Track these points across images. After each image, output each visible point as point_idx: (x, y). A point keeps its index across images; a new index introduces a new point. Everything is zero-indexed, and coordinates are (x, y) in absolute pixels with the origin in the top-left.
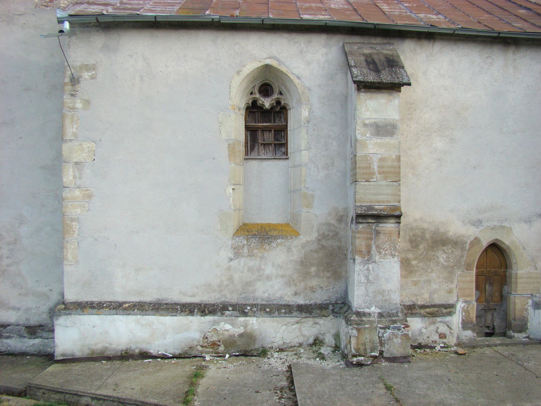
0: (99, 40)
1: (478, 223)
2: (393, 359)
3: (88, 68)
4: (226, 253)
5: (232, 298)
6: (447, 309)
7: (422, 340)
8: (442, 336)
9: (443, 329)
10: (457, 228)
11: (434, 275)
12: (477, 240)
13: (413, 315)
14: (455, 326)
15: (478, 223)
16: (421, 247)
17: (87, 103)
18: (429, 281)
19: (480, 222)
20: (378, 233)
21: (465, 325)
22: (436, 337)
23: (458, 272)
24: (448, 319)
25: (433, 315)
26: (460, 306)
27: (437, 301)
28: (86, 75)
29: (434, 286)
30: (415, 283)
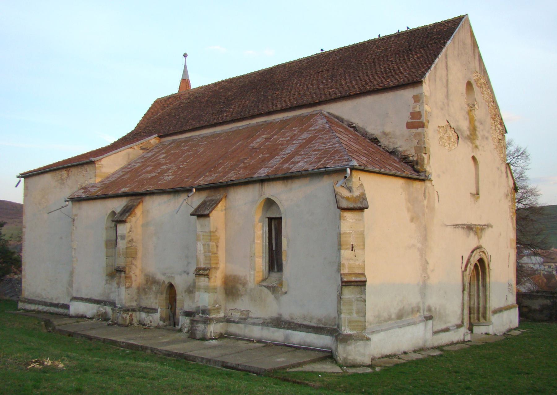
0: (77, 205)
1: (164, 274)
2: (120, 325)
3: (76, 215)
4: (104, 282)
5: (105, 299)
6: (154, 310)
7: (145, 322)
8: (151, 322)
9: (151, 319)
10: (160, 277)
11: (151, 296)
12: (164, 282)
13: (143, 311)
14: (155, 318)
15: (164, 274)
16: (149, 283)
17: (76, 228)
18: (150, 298)
19: (165, 273)
20: (121, 277)
21: (162, 319)
22: (149, 322)
23: (159, 295)
24: (152, 314)
25: (148, 312)
26: (159, 310)
27: (153, 307)
28: (76, 218)
29: (152, 300)
30: (147, 298)
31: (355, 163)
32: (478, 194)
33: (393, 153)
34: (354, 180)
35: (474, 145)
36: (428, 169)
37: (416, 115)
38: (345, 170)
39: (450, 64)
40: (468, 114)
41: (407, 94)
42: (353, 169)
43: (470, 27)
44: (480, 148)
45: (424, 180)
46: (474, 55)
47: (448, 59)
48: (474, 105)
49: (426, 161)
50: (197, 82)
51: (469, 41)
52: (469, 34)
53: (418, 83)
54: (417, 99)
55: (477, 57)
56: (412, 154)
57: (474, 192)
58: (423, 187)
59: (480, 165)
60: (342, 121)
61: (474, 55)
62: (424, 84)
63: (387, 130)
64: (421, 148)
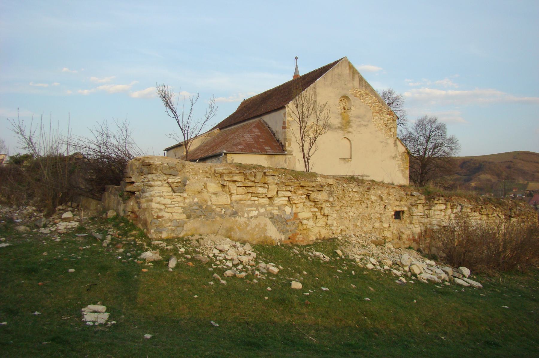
31: (225, 151)
32: (351, 158)
33: (278, 141)
34: (228, 157)
35: (345, 132)
36: (288, 148)
37: (284, 123)
38: (222, 155)
39: (318, 90)
40: (341, 114)
41: (282, 112)
42: (225, 154)
43: (349, 63)
44: (354, 132)
45: (285, 155)
46: (353, 78)
47: (317, 89)
48: (350, 108)
49: (287, 145)
50: (302, 73)
51: (346, 71)
52: (348, 68)
53: (283, 107)
54: (285, 114)
55: (357, 79)
56: (282, 141)
57: (349, 157)
58: (284, 159)
59: (352, 143)
60: (267, 124)
61: (353, 78)
62: (287, 108)
63: (277, 130)
64: (285, 139)
